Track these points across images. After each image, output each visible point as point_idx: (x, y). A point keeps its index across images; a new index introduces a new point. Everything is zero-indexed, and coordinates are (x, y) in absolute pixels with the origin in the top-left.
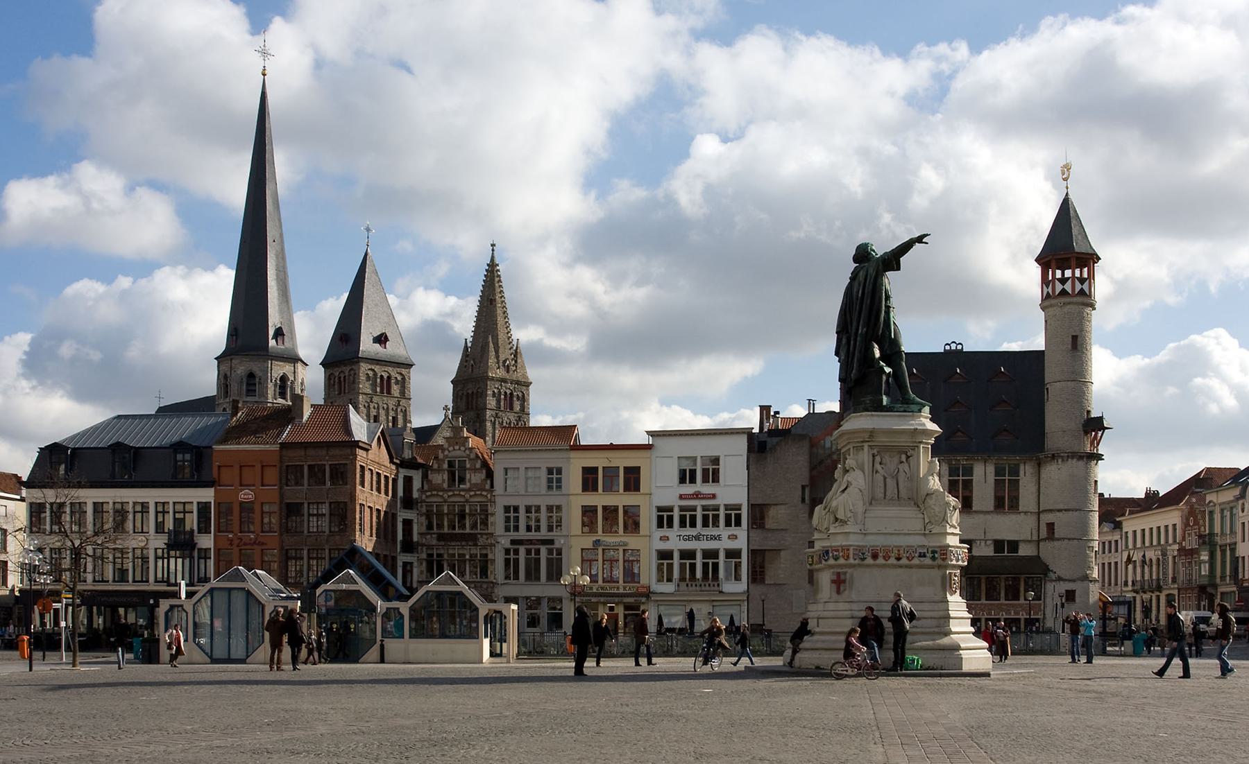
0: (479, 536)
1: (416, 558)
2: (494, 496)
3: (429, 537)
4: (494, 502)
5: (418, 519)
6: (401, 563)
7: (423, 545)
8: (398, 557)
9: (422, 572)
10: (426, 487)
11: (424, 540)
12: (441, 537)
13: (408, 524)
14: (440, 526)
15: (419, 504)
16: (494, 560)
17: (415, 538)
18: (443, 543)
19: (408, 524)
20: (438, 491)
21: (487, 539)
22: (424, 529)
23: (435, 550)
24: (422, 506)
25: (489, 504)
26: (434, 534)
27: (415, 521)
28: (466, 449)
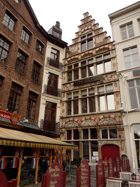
0: (104, 76)
1: (60, 101)
2: (114, 45)
3: (68, 85)
4: (115, 49)
5: (62, 75)
6: (45, 102)
7: (64, 92)
8: (42, 97)
9: (63, 111)
10: (68, 56)
11: (66, 88)
12: (76, 84)
13: (53, 79)
14: (77, 76)
15: (63, 67)
16: (119, 92)
17: (60, 87)
18: (78, 87)
19: (53, 79)
20: (75, 56)
21: (111, 77)
22: (66, 81)
23: (72, 94)
24: (65, 68)
25: (111, 52)
26: (72, 82)
27: (60, 76)
28: (92, 27)
